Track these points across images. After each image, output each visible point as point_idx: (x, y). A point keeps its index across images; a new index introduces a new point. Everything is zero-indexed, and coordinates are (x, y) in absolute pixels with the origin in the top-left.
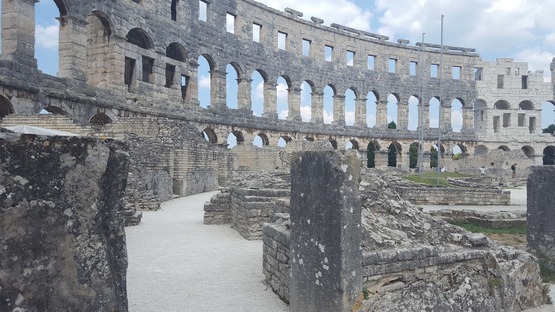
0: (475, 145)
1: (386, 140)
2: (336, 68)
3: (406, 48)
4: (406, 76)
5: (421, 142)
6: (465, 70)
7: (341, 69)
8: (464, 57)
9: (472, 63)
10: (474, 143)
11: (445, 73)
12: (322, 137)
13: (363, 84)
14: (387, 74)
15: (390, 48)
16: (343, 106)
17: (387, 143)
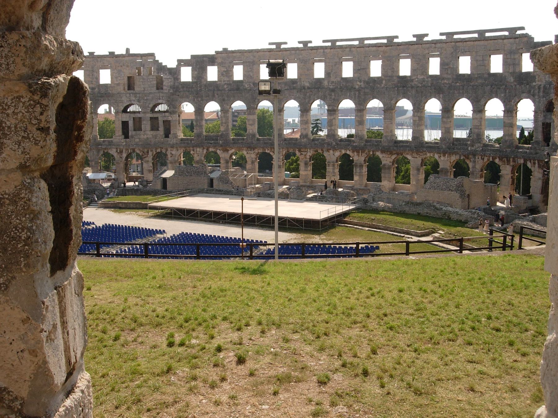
0: (512, 164)
1: (388, 153)
2: (326, 83)
3: (421, 44)
4: (421, 77)
5: (436, 156)
6: (508, 59)
7: (333, 82)
8: (505, 41)
9: (518, 48)
10: (511, 160)
11: (477, 66)
12: (305, 152)
13: (359, 93)
14: (395, 78)
15: (399, 47)
16: (334, 120)
17: (390, 156)
